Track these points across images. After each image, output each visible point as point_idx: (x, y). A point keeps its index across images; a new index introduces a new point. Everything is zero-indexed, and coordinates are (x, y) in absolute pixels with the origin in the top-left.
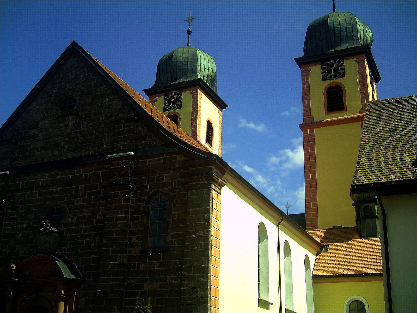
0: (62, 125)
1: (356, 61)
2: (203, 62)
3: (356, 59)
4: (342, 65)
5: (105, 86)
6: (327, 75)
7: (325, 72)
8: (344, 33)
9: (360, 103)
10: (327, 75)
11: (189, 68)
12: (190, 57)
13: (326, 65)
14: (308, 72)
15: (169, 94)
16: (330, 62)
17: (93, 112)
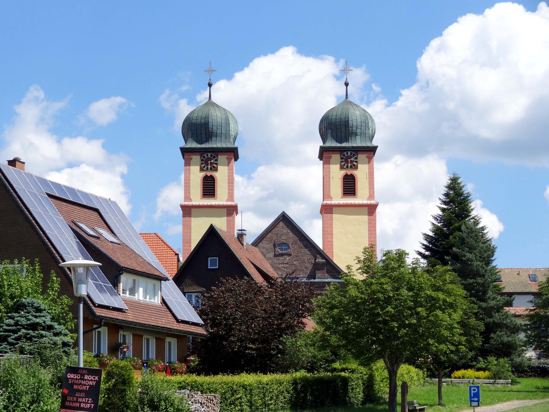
0: (281, 258)
1: (367, 157)
2: (232, 127)
3: (367, 155)
4: (356, 158)
5: (306, 241)
6: (345, 164)
7: (343, 162)
8: (359, 131)
9: (368, 192)
10: (345, 164)
11: (223, 132)
12: (223, 122)
13: (344, 155)
14: (329, 158)
15: (205, 155)
16: (347, 153)
17: (300, 254)
